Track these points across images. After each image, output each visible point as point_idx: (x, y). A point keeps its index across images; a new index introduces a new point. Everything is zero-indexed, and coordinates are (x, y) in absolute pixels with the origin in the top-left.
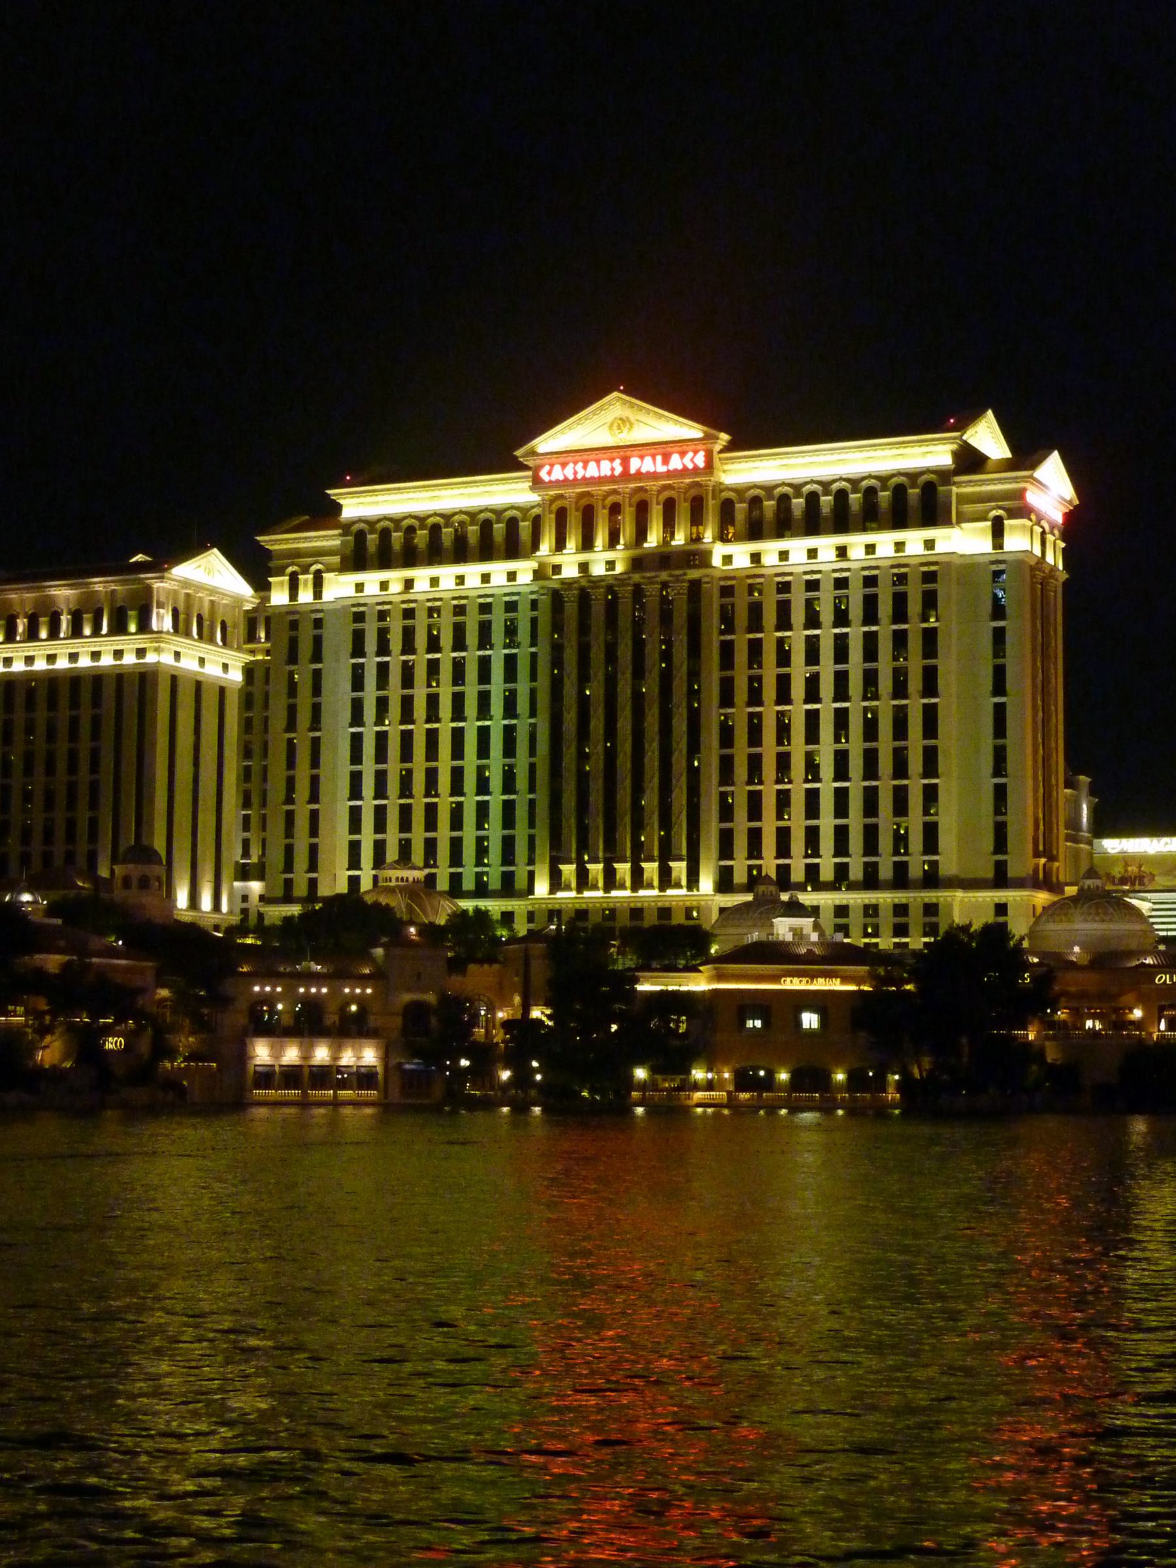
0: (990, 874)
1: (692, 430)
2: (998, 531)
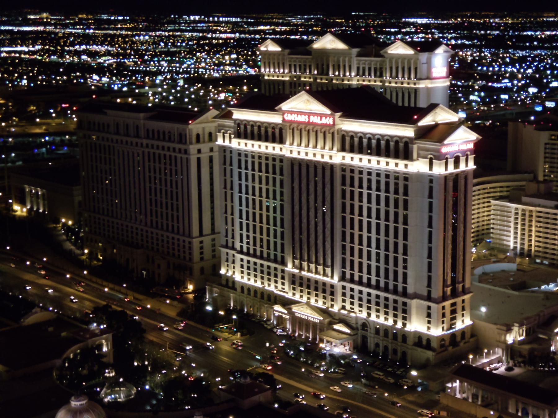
0: (425, 294)
1: (328, 111)
2: (431, 164)
